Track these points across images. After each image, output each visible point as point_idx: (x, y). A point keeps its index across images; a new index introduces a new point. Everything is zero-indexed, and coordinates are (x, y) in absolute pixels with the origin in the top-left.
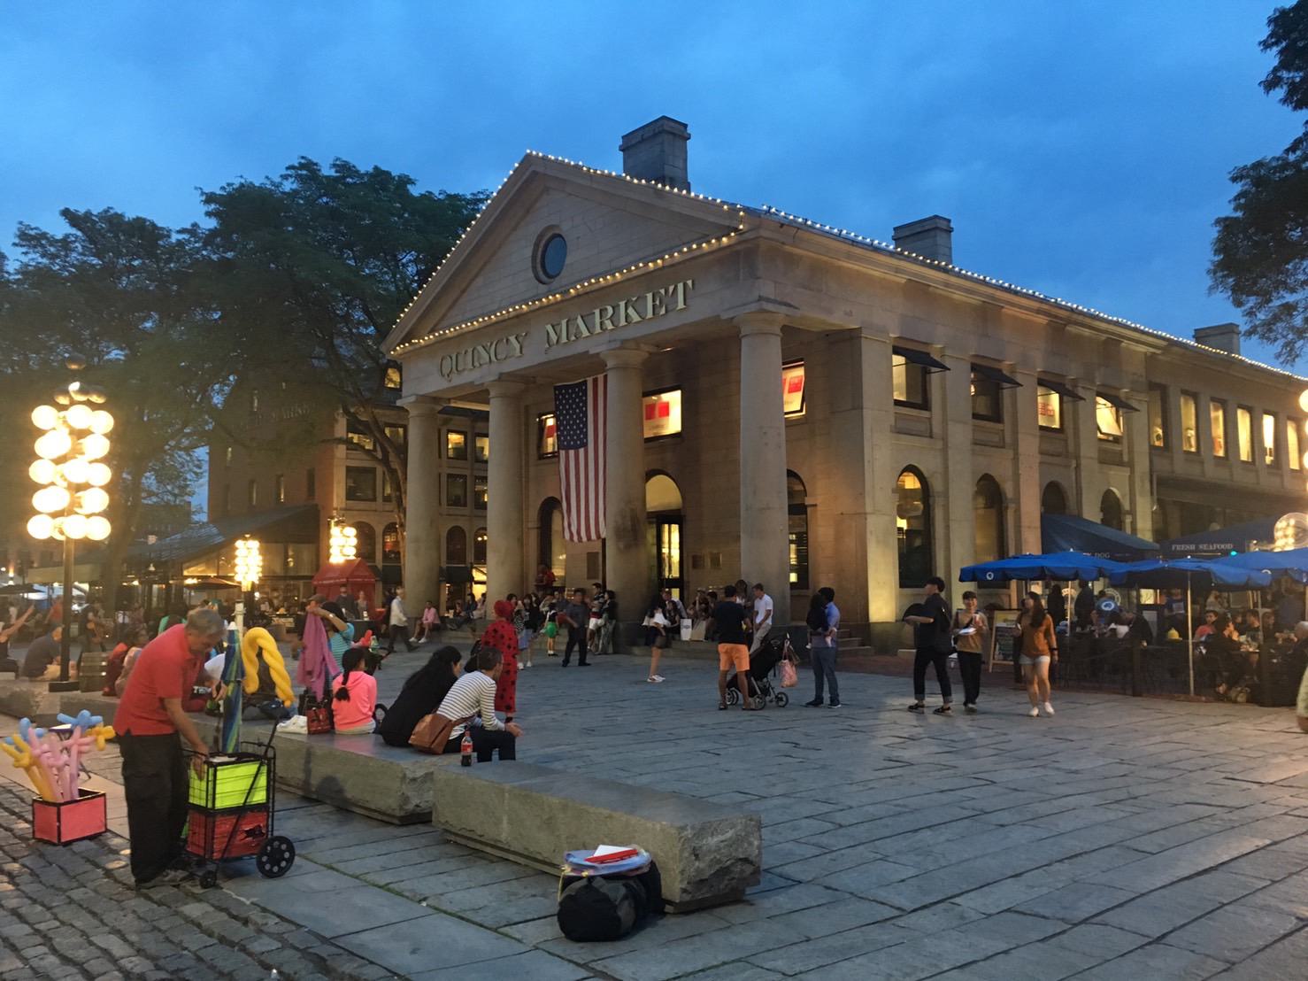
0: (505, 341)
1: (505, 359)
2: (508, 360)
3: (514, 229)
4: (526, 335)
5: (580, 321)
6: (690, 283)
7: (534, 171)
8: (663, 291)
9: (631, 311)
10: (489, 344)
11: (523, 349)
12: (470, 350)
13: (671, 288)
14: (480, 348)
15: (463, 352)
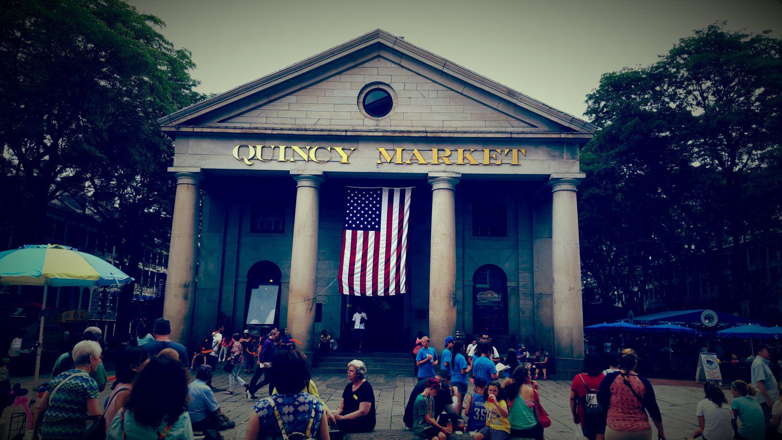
0: (329, 149)
1: (328, 161)
2: (329, 163)
3: (339, 73)
4: (354, 150)
5: (416, 152)
6: (523, 151)
7: (379, 43)
8: (499, 151)
9: (467, 155)
10: (308, 148)
11: (349, 159)
12: (282, 148)
13: (506, 151)
14: (296, 148)
15: (273, 147)
